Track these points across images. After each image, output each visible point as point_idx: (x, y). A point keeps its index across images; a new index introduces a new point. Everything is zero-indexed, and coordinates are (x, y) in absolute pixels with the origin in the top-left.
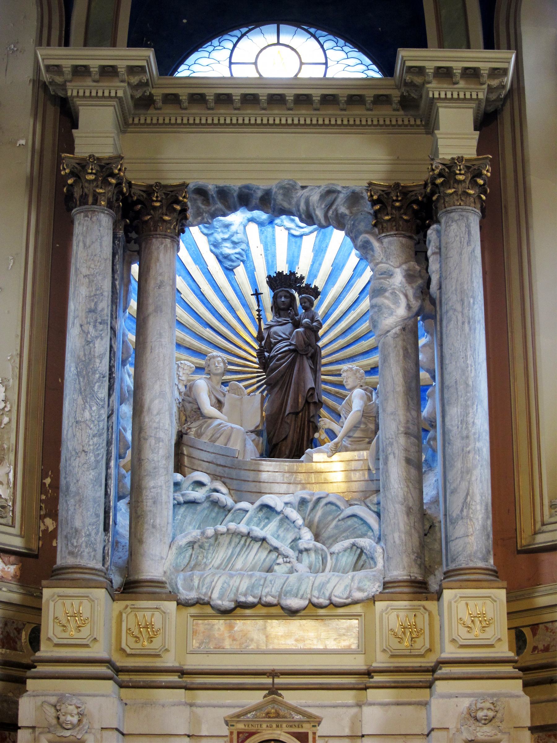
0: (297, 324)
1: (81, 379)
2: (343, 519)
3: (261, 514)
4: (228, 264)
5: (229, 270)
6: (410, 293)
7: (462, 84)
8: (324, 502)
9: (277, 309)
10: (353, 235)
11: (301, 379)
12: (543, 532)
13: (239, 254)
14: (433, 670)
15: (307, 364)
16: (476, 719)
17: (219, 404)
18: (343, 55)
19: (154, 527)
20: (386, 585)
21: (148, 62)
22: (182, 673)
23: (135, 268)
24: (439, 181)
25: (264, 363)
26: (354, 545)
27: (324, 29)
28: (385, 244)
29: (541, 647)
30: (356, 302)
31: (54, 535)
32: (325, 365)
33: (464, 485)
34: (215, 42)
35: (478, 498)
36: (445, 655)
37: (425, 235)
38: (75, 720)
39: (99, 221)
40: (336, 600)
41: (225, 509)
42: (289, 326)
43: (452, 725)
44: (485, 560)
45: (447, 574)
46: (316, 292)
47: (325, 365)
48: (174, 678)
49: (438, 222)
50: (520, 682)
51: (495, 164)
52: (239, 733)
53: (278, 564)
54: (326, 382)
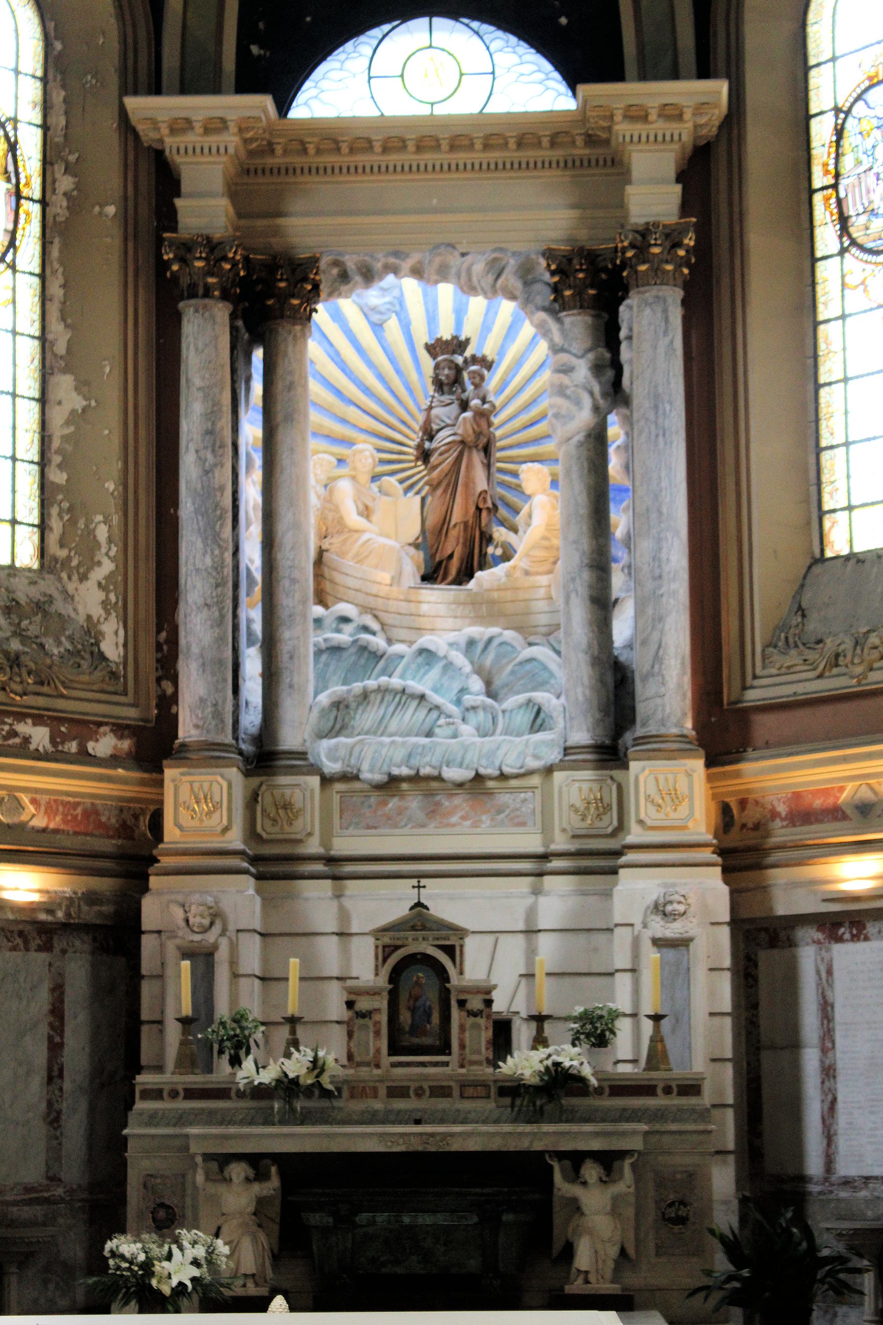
0: (464, 406)
1: (200, 518)
2: (521, 663)
3: (420, 660)
4: (375, 318)
5: (377, 327)
6: (597, 389)
8: (495, 643)
9: (439, 385)
11: (469, 483)
12: (752, 687)
13: (390, 303)
15: (477, 458)
16: (665, 914)
17: (366, 512)
19: (291, 686)
20: (567, 750)
21: (265, 111)
22: (331, 860)
23: (258, 354)
26: (529, 701)
27: (491, 23)
29: (750, 825)
32: (503, 449)
33: (655, 636)
34: (349, 46)
35: (672, 650)
36: (630, 839)
39: (213, 318)
40: (507, 770)
41: (376, 656)
42: (455, 408)
43: (637, 920)
45: (638, 741)
46: (488, 365)
47: (503, 449)
48: (319, 867)
50: (718, 870)
52: (384, 947)
53: (440, 726)
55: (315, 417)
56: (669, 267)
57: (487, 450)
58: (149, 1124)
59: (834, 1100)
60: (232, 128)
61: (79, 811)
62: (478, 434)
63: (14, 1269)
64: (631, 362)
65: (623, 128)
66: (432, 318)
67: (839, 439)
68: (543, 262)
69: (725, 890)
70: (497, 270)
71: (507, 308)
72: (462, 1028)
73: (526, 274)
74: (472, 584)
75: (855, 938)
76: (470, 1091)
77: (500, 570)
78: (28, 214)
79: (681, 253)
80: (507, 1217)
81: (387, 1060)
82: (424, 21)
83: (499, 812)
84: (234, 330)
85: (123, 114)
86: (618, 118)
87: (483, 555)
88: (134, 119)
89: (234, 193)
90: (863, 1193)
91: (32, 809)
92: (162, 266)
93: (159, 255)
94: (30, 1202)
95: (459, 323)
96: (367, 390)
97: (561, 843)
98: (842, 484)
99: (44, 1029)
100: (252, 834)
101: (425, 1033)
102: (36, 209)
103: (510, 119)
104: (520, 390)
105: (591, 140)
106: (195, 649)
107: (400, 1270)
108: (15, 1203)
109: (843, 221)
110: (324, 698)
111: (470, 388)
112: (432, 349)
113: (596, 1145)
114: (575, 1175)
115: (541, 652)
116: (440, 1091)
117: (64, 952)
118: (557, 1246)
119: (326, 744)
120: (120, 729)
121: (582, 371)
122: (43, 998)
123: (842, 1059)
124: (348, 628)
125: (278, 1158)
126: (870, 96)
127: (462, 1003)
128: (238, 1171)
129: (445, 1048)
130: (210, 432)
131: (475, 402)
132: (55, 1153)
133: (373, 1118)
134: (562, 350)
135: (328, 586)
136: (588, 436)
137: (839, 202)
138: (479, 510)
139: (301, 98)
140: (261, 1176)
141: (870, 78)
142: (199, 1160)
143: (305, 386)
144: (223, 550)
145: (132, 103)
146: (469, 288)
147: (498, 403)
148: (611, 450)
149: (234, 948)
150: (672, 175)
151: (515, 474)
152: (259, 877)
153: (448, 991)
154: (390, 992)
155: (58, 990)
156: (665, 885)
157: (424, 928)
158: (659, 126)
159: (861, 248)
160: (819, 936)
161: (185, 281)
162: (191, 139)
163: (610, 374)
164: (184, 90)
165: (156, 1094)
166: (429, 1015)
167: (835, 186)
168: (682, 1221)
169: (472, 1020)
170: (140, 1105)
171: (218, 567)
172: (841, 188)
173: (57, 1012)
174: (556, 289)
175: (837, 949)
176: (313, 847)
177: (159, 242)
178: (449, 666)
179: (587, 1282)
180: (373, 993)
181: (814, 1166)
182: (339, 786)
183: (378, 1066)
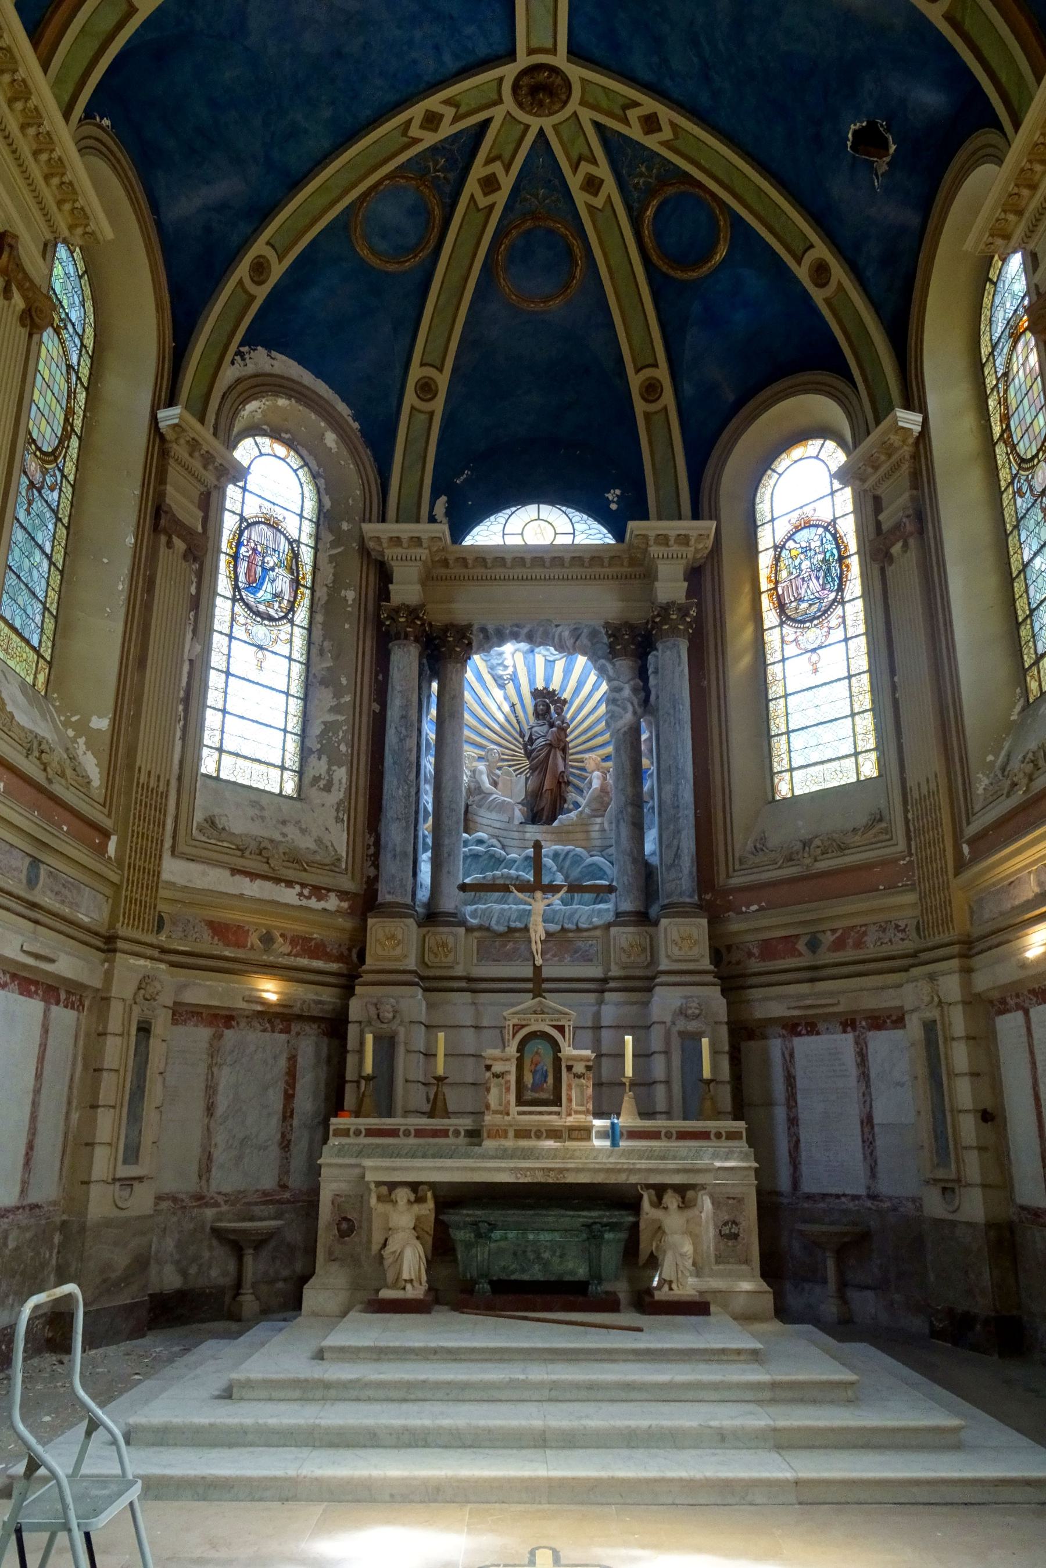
0: (552, 725)
3: (526, 863)
6: (636, 702)
7: (675, 548)
8: (571, 854)
9: (537, 714)
11: (556, 765)
14: (654, 978)
15: (559, 754)
16: (686, 1016)
17: (495, 784)
18: (586, 527)
19: (449, 872)
20: (618, 915)
21: (444, 533)
22: (469, 979)
23: (435, 685)
24: (658, 620)
25: (528, 754)
27: (572, 508)
28: (617, 667)
30: (595, 708)
31: (376, 879)
32: (572, 754)
33: (675, 842)
34: (492, 518)
35: (686, 851)
36: (662, 968)
37: (647, 659)
38: (390, 1016)
39: (409, 651)
40: (582, 926)
42: (545, 728)
44: (691, 896)
45: (664, 907)
46: (565, 702)
47: (572, 754)
48: (463, 984)
49: (656, 649)
50: (718, 988)
51: (699, 605)
52: (514, 1026)
54: (572, 767)
55: (467, 732)
56: (681, 627)
57: (564, 750)
58: (338, 1155)
59: (798, 1141)
61: (313, 943)
62: (560, 740)
63: (251, 1251)
64: (657, 685)
65: (655, 550)
67: (783, 729)
68: (603, 631)
70: (576, 633)
71: (581, 660)
73: (593, 634)
74: (555, 824)
75: (809, 1033)
76: (575, 1134)
77: (573, 815)
78: (302, 594)
79: (688, 620)
80: (609, 1236)
81: (514, 1109)
83: (576, 952)
84: (421, 664)
86: (651, 543)
87: (562, 808)
90: (822, 1205)
91: (281, 940)
93: (379, 616)
94: (265, 1203)
97: (615, 971)
98: (785, 757)
99: (281, 1085)
100: (423, 963)
101: (543, 1090)
102: (308, 592)
104: (583, 721)
107: (526, 1277)
108: (256, 1204)
109: (781, 607)
112: (536, 694)
115: (598, 859)
117: (298, 1034)
119: (469, 908)
120: (343, 895)
121: (627, 692)
122: (283, 1063)
124: (485, 845)
125: (432, 1185)
126: (797, 537)
128: (403, 1195)
130: (403, 717)
132: (285, 1170)
133: (504, 1154)
134: (614, 680)
135: (471, 825)
136: (631, 728)
137: (778, 596)
138: (559, 783)
140: (420, 1200)
141: (796, 527)
142: (373, 1186)
143: (463, 716)
144: (410, 787)
145: (366, 527)
150: (682, 577)
152: (426, 990)
153: (559, 1060)
154: (518, 1059)
155: (292, 1059)
156: (686, 997)
157: (543, 1013)
158: (675, 548)
159: (794, 620)
161: (393, 631)
163: (643, 694)
165: (346, 1133)
166: (546, 1076)
167: (775, 589)
168: (735, 1236)
170: (334, 1141)
171: (407, 797)
173: (291, 1074)
174: (611, 646)
175: (797, 1041)
176: (459, 971)
179: (671, 1289)
182: (477, 934)
183: (508, 1114)
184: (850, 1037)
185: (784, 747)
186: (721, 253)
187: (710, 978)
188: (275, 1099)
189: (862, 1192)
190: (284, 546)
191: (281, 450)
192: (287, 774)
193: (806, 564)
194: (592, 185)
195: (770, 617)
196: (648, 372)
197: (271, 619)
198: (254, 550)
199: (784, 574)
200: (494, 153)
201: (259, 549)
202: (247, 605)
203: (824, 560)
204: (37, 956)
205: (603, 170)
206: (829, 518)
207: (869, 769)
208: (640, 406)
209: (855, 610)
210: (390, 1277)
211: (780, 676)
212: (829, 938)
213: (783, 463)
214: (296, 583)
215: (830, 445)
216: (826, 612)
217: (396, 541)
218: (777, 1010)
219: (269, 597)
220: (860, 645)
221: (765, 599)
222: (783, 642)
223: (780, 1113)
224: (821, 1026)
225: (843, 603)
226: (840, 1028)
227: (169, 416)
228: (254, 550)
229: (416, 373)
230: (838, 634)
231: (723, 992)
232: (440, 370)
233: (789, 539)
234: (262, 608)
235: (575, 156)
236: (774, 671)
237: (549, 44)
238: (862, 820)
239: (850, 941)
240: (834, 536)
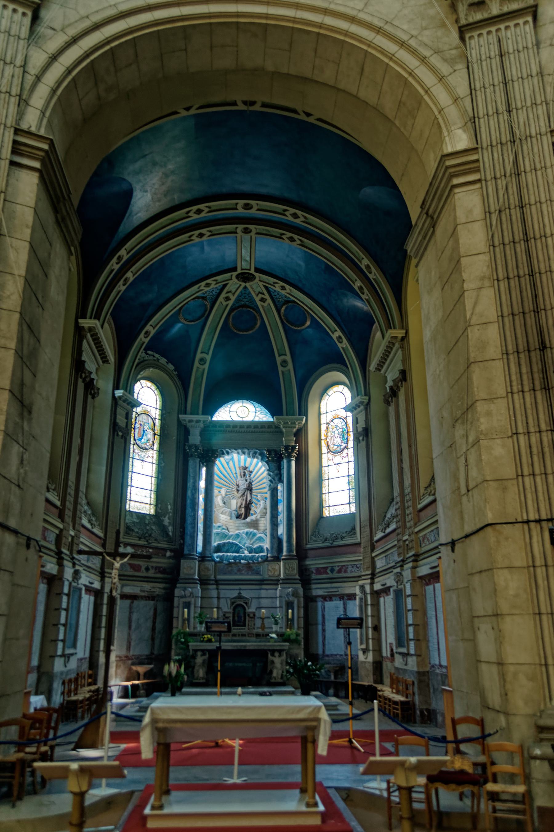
4: (227, 461)
5: (228, 463)
10: (262, 459)
15: (249, 492)
23: (204, 470)
34: (226, 405)
42: (245, 481)
60: (202, 422)
62: (249, 487)
66: (239, 461)
69: (302, 589)
70: (255, 453)
72: (249, 621)
80: (258, 664)
82: (241, 401)
85: (178, 417)
88: (181, 419)
89: (201, 435)
90: (331, 658)
92: (185, 450)
95: (245, 463)
96: (225, 477)
99: (152, 619)
103: (259, 422)
105: (276, 427)
106: (189, 533)
109: (328, 446)
110: (216, 544)
111: (248, 477)
113: (278, 648)
114: (273, 655)
116: (243, 635)
118: (268, 671)
119: (215, 555)
120: (171, 551)
123: (327, 628)
124: (220, 529)
127: (249, 615)
129: (245, 625)
131: (249, 480)
139: (215, 415)
140: (204, 654)
145: (180, 416)
146: (249, 457)
147: (253, 479)
148: (279, 492)
149: (195, 601)
151: (257, 496)
155: (155, 610)
160: (322, 600)
161: (190, 454)
162: (193, 424)
163: (279, 476)
164: (191, 414)
169: (250, 619)
172: (328, 440)
177: (185, 445)
178: (242, 538)
180: (229, 613)
181: (320, 652)
184: (342, 602)
185: (327, 498)
186: (308, 323)
187: (298, 581)
188: (149, 624)
189: (343, 653)
190: (150, 421)
191: (149, 384)
192: (152, 506)
193: (336, 432)
194: (263, 300)
195: (324, 449)
196: (283, 357)
197: (146, 449)
198: (141, 424)
199: (329, 434)
200: (229, 290)
201: (142, 423)
202: (138, 445)
203: (343, 432)
204: (92, 583)
205: (267, 296)
206: (345, 416)
207: (353, 510)
208: (280, 368)
209: (351, 451)
210: (196, 675)
211: (327, 472)
212: (337, 569)
213: (331, 392)
214: (155, 434)
215: (346, 388)
216: (342, 450)
217: (191, 421)
218: (320, 592)
219: (145, 441)
220: (352, 465)
221: (323, 442)
222: (328, 459)
223: (320, 627)
224: (334, 598)
225: (348, 449)
226: (339, 599)
227: (119, 393)
228: (141, 424)
229: (199, 356)
230: (346, 460)
231: (302, 587)
232: (208, 354)
233: (332, 421)
234: (143, 446)
235: (257, 293)
236: (325, 469)
237: (248, 268)
238: (349, 529)
239: (343, 570)
240: (346, 423)
